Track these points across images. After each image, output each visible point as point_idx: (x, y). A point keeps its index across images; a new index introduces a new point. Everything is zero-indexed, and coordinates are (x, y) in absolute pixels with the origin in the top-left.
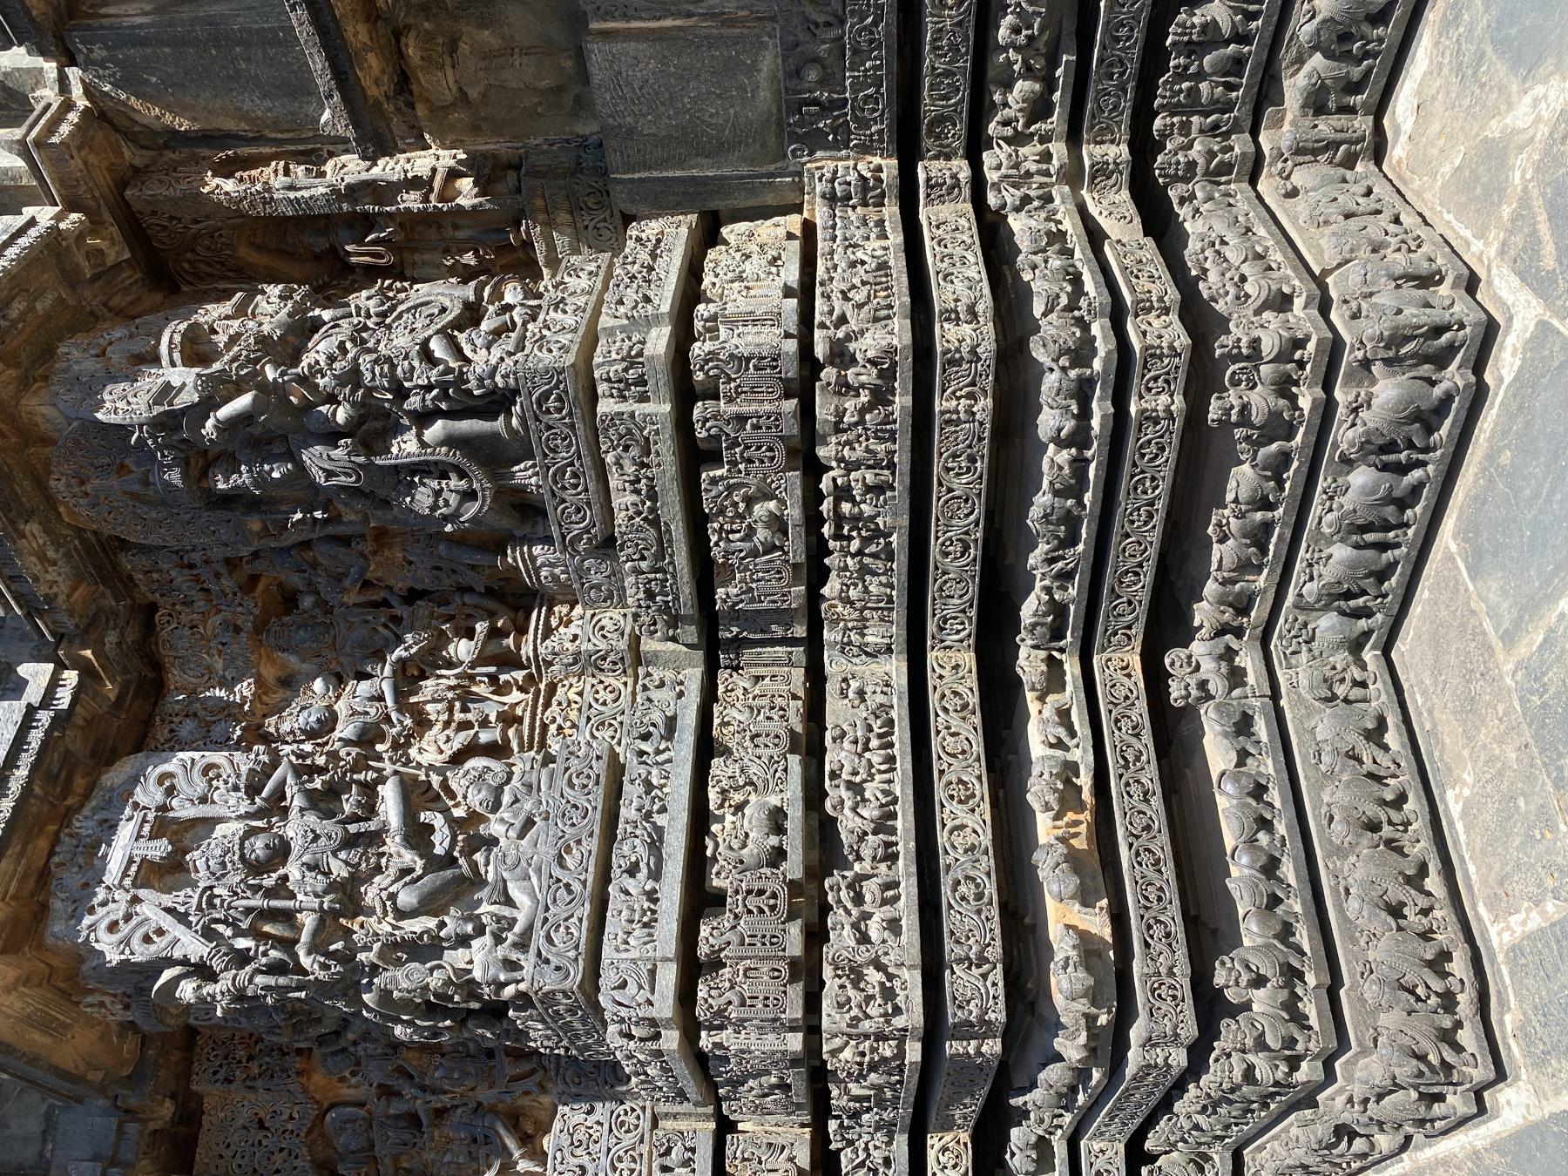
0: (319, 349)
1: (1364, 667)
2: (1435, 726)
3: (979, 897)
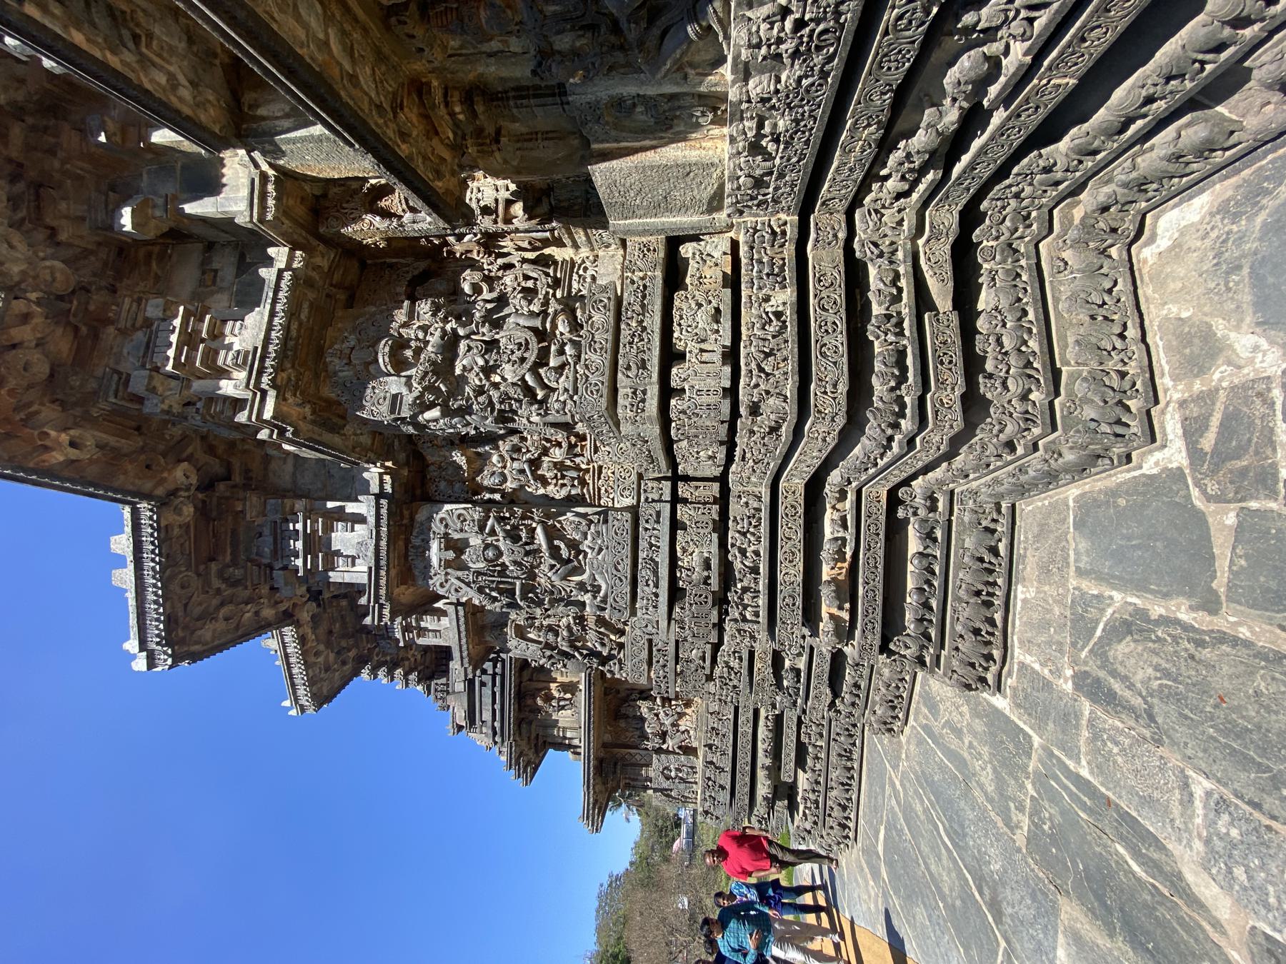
1: (999, 511)
3: (794, 605)
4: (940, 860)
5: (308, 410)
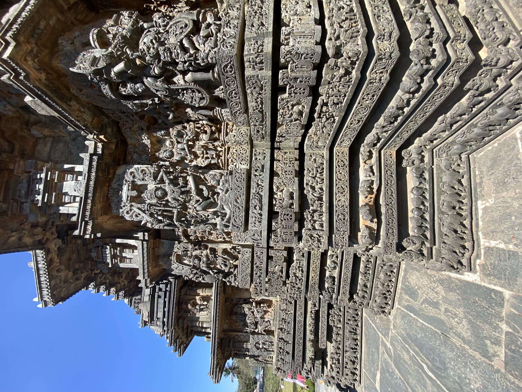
0: (145, 42)
2: (482, 182)
3: (344, 219)
4: (425, 387)
5: (43, 76)
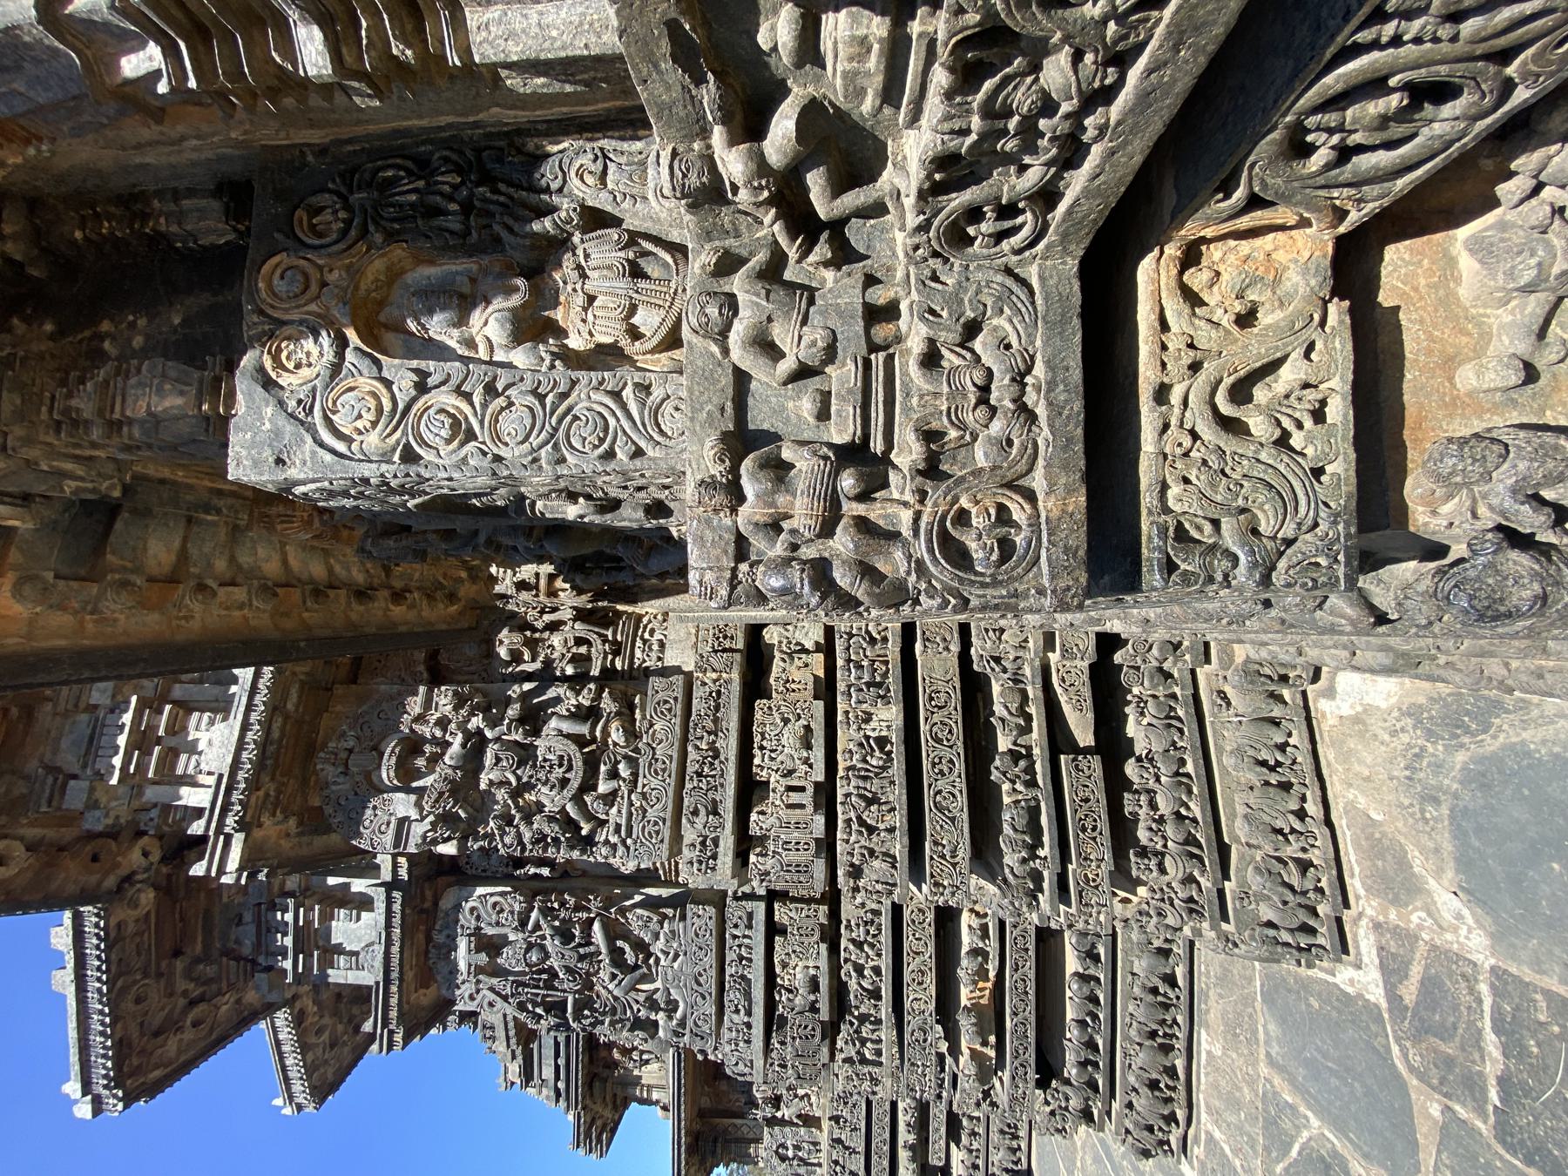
5: (292, 822)
